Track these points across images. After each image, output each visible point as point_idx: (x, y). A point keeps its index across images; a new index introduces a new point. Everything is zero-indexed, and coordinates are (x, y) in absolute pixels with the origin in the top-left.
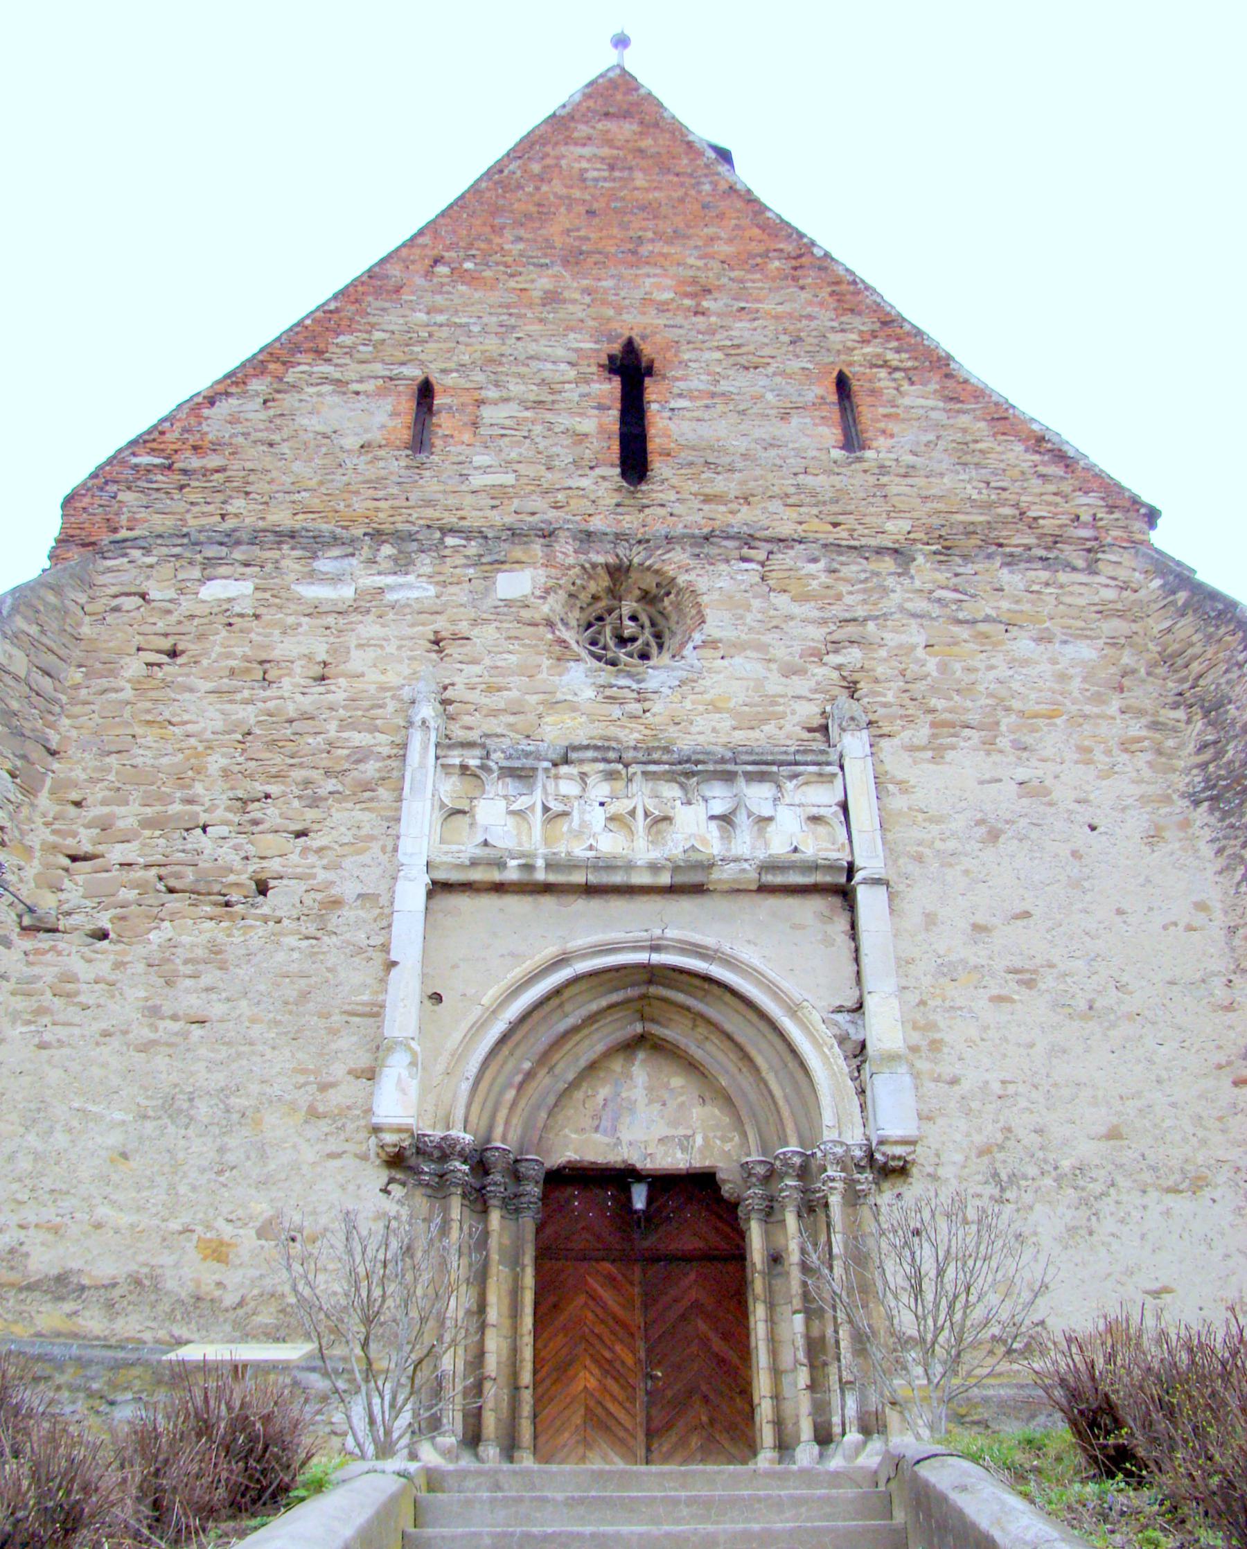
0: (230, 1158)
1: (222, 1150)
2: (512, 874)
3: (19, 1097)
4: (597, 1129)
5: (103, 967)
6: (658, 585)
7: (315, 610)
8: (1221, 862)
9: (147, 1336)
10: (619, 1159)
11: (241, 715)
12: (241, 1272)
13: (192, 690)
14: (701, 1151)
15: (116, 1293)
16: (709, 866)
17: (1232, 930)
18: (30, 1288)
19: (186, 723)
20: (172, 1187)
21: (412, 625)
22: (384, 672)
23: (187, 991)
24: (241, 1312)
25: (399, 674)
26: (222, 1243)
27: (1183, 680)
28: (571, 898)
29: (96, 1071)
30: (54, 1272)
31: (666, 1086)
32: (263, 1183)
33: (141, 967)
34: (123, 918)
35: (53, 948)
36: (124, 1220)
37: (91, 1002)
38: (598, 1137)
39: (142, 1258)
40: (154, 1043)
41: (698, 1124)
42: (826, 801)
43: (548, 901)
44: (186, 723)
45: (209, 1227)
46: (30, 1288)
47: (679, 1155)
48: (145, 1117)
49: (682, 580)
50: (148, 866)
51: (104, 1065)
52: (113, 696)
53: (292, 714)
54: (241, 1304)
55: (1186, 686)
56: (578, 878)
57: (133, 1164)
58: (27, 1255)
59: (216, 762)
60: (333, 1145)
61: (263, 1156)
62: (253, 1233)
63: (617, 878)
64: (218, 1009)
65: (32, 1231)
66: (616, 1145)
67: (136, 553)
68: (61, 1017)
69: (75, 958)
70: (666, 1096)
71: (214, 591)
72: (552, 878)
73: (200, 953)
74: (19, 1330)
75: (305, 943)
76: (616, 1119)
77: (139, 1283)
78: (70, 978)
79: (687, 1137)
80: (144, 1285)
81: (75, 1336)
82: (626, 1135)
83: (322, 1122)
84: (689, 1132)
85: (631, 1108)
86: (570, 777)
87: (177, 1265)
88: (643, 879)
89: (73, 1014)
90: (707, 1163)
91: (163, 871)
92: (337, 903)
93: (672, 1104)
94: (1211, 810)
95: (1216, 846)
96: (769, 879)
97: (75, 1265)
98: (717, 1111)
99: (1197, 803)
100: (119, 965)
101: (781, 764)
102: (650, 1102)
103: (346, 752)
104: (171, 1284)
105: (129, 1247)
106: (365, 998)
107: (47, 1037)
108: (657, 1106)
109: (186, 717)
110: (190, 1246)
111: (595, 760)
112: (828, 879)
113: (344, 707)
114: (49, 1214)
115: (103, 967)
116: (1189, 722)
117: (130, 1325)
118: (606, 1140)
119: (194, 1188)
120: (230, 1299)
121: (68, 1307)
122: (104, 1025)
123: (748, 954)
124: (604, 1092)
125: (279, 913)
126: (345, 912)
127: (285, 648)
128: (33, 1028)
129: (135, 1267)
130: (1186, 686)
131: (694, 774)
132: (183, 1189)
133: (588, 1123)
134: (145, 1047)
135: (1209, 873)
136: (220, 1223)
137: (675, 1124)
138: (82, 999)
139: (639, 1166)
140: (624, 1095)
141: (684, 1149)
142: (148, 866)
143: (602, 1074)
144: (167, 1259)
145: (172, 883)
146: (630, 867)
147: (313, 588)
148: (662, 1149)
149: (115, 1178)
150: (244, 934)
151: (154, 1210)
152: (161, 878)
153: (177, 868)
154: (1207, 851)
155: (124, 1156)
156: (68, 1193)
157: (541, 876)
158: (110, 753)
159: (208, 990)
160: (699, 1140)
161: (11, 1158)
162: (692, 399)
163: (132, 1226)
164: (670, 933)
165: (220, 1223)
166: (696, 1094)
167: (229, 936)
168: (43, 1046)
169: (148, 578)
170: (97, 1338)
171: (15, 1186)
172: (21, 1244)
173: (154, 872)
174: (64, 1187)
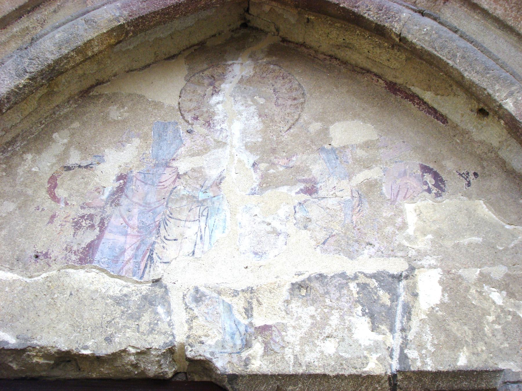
4: (86, 257)
10: (157, 342)
14: (437, 322)
31: (320, 144)
38: (83, 277)
41: (423, 243)
47: (362, 331)
66: (148, 301)
70: (317, 168)
76: (155, 228)
79: (390, 281)
82: (181, 269)
84: (396, 266)
85: (206, 195)
90: (462, 361)
93: (338, 190)
98: (483, 209)
102: (267, 183)
108: (291, 194)
118: (115, 287)
124: (117, 159)
133: (57, 237)
137: (348, 242)
139: (222, 364)
140: (183, 165)
141: (378, 316)
143: (115, 113)
148: (304, 313)
160: (430, 290)
166: (414, 164)
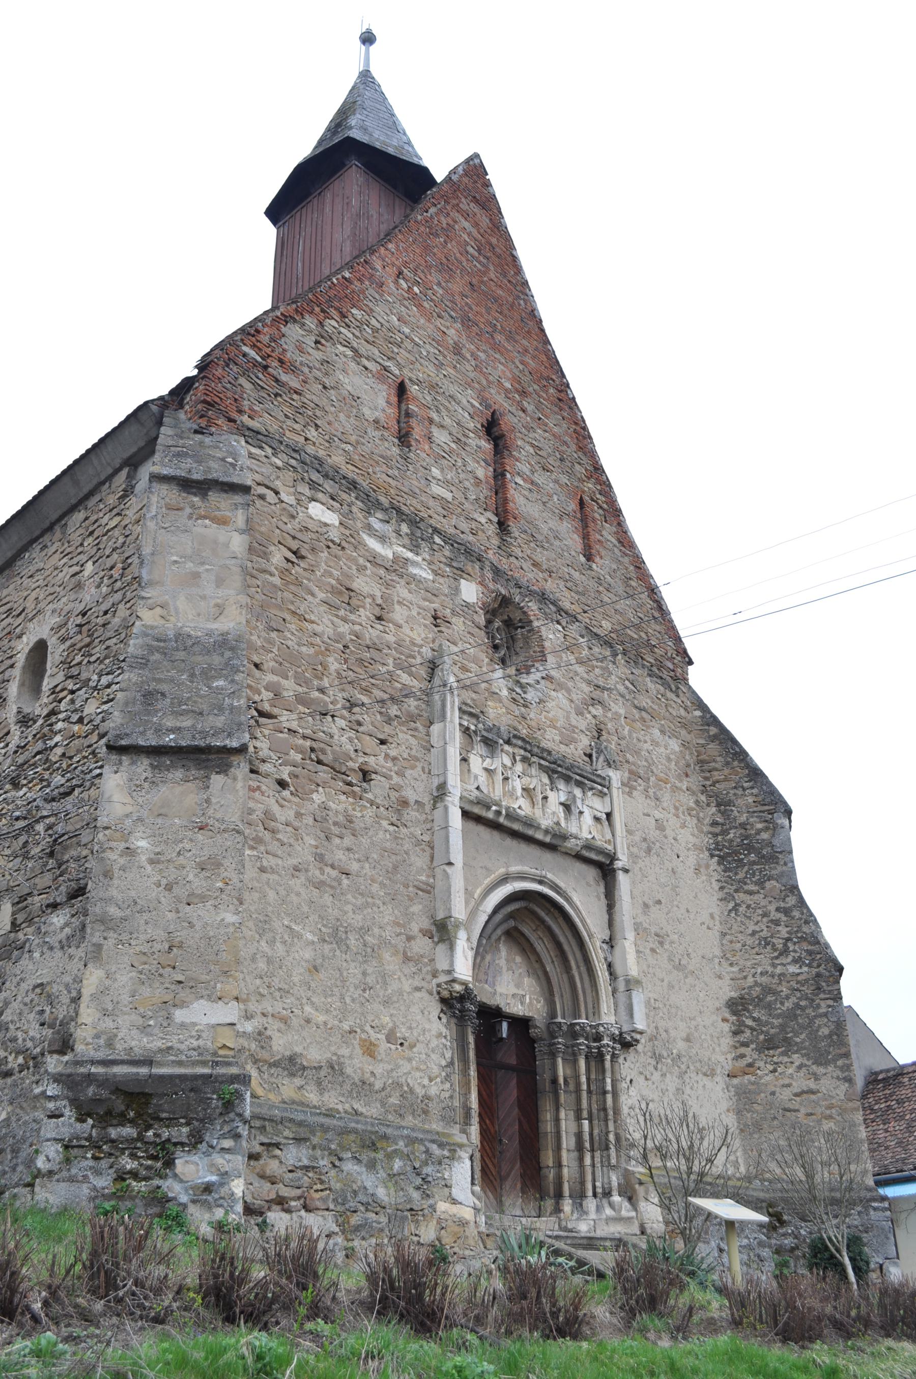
0: (370, 980)
1: (364, 974)
2: (490, 815)
3: (252, 908)
5: (290, 814)
6: (520, 620)
7: (374, 559)
8: (721, 895)
9: (340, 1107)
11: (341, 630)
12: (381, 1065)
13: (313, 595)
15: (323, 1073)
16: (564, 837)
17: (724, 935)
18: (275, 1064)
19: (313, 622)
20: (342, 997)
21: (424, 599)
22: (412, 629)
23: (338, 847)
24: (383, 1094)
25: (419, 635)
26: (371, 1043)
27: (706, 779)
28: (505, 836)
29: (293, 897)
30: (288, 1053)
32: (386, 1003)
33: (310, 821)
34: (296, 777)
35: (259, 788)
36: (321, 1018)
37: (285, 840)
39: (333, 1049)
40: (323, 883)
42: (600, 809)
43: (496, 835)
44: (313, 622)
45: (363, 1031)
46: (275, 1064)
48: (324, 941)
49: (536, 624)
50: (305, 737)
51: (298, 894)
52: (267, 576)
53: (368, 642)
54: (383, 1089)
55: (708, 783)
56: (516, 826)
57: (321, 976)
58: (270, 1038)
59: (334, 665)
60: (417, 983)
61: (385, 983)
62: (383, 1037)
63: (530, 832)
64: (354, 867)
65: (270, 1020)
67: (269, 451)
68: (269, 848)
69: (273, 801)
71: (317, 511)
72: (507, 823)
73: (341, 818)
74: (271, 1096)
75: (392, 828)
77: (332, 1068)
78: (274, 820)
80: (335, 1068)
81: (302, 1104)
83: (411, 964)
86: (507, 753)
87: (351, 1057)
88: (539, 836)
89: (274, 846)
91: (315, 745)
92: (405, 803)
94: (719, 863)
95: (720, 884)
96: (586, 853)
97: (298, 1049)
99: (712, 856)
100: (299, 815)
101: (589, 780)
103: (399, 686)
104: (349, 1071)
105: (326, 1039)
106: (424, 878)
107: (265, 863)
109: (313, 618)
110: (356, 1042)
111: (521, 748)
112: (600, 858)
113: (395, 649)
114: (278, 1007)
115: (290, 814)
116: (708, 805)
117: (332, 1100)
119: (353, 1000)
120: (378, 1085)
121: (298, 1081)
122: (295, 861)
123: (576, 898)
125: (378, 801)
126: (409, 810)
127: (361, 584)
128: (255, 853)
129: (330, 1055)
130: (708, 783)
131: (557, 772)
132: (348, 1000)
134: (319, 885)
135: (715, 898)
136: (368, 1028)
138: (280, 836)
142: (305, 737)
144: (345, 1051)
145: (322, 757)
146: (538, 828)
147: (372, 540)
149: (313, 985)
150: (361, 811)
151: (335, 1013)
152: (312, 750)
153: (322, 745)
154: (716, 886)
155: (316, 968)
156: (288, 992)
157: (501, 820)
158: (274, 630)
159: (348, 849)
161: (253, 959)
162: (524, 480)
163: (325, 1023)
164: (549, 876)
165: (368, 1028)
167: (354, 810)
168: (262, 870)
169: (278, 477)
170: (315, 1107)
171: (258, 981)
172: (266, 1029)
173: (308, 743)
174: (286, 987)
